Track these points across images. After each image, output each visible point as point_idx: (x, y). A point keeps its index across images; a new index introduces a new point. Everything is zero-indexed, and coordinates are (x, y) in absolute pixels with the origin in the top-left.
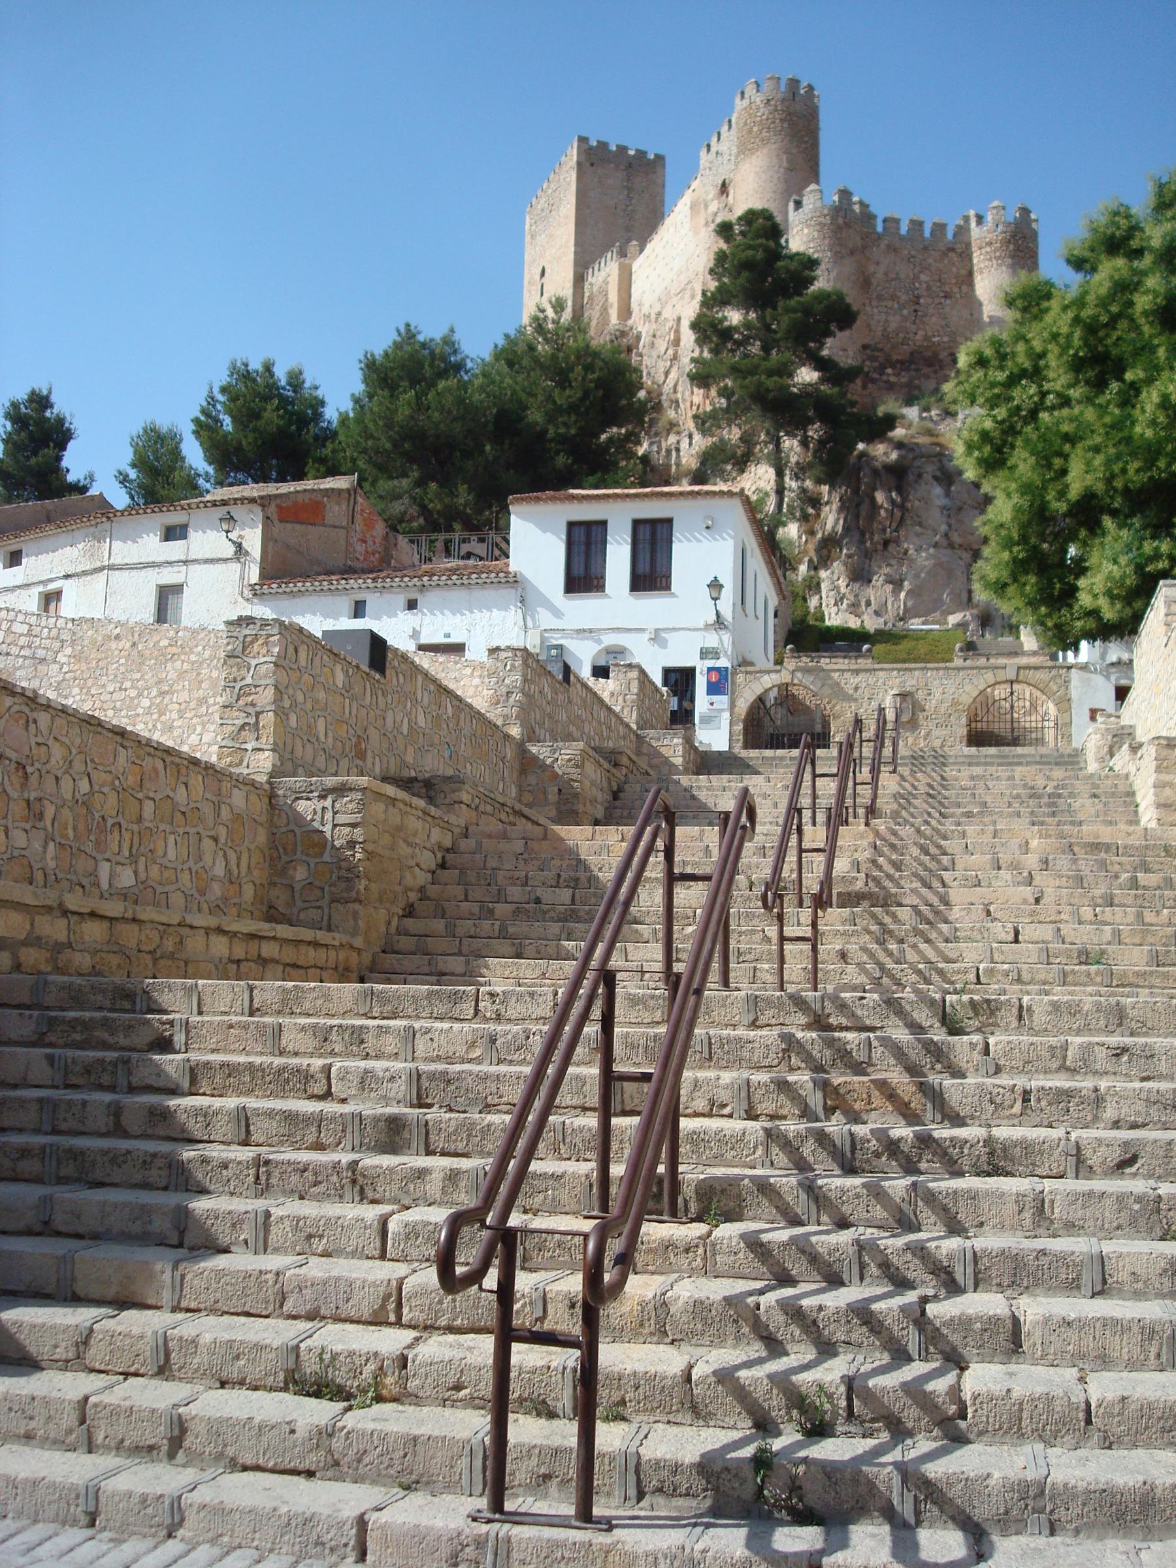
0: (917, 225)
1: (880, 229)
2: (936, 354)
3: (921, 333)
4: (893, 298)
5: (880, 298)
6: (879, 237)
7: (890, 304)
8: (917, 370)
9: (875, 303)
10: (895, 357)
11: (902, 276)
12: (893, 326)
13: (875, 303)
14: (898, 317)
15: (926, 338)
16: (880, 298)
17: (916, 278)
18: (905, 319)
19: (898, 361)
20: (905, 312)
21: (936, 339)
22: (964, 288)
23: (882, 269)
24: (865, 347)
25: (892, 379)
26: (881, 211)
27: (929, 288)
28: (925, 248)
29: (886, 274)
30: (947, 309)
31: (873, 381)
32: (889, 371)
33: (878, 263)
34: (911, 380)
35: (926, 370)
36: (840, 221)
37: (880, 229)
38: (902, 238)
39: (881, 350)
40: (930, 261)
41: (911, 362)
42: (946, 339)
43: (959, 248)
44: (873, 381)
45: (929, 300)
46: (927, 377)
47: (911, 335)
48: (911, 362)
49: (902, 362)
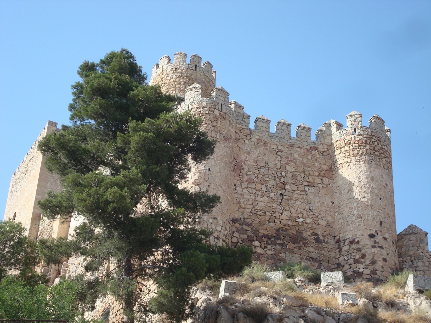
0: (284, 126)
1: (252, 126)
2: (300, 233)
3: (286, 213)
4: (262, 182)
5: (249, 181)
6: (251, 132)
7: (259, 186)
8: (282, 245)
9: (245, 185)
10: (262, 232)
11: (271, 165)
12: (261, 205)
13: (245, 185)
14: (265, 198)
16: (249, 181)
17: (282, 168)
18: (273, 200)
19: (264, 236)
20: (272, 195)
21: (301, 220)
22: (326, 180)
24: (234, 221)
26: (253, 111)
27: (294, 177)
28: (292, 145)
30: (311, 196)
32: (256, 243)
33: (249, 153)
34: (277, 253)
35: (291, 246)
37: (252, 126)
38: (271, 135)
39: (250, 225)
40: (296, 156)
42: (309, 221)
43: (321, 148)
45: (295, 188)
46: (292, 252)
47: (277, 214)
48: (277, 237)
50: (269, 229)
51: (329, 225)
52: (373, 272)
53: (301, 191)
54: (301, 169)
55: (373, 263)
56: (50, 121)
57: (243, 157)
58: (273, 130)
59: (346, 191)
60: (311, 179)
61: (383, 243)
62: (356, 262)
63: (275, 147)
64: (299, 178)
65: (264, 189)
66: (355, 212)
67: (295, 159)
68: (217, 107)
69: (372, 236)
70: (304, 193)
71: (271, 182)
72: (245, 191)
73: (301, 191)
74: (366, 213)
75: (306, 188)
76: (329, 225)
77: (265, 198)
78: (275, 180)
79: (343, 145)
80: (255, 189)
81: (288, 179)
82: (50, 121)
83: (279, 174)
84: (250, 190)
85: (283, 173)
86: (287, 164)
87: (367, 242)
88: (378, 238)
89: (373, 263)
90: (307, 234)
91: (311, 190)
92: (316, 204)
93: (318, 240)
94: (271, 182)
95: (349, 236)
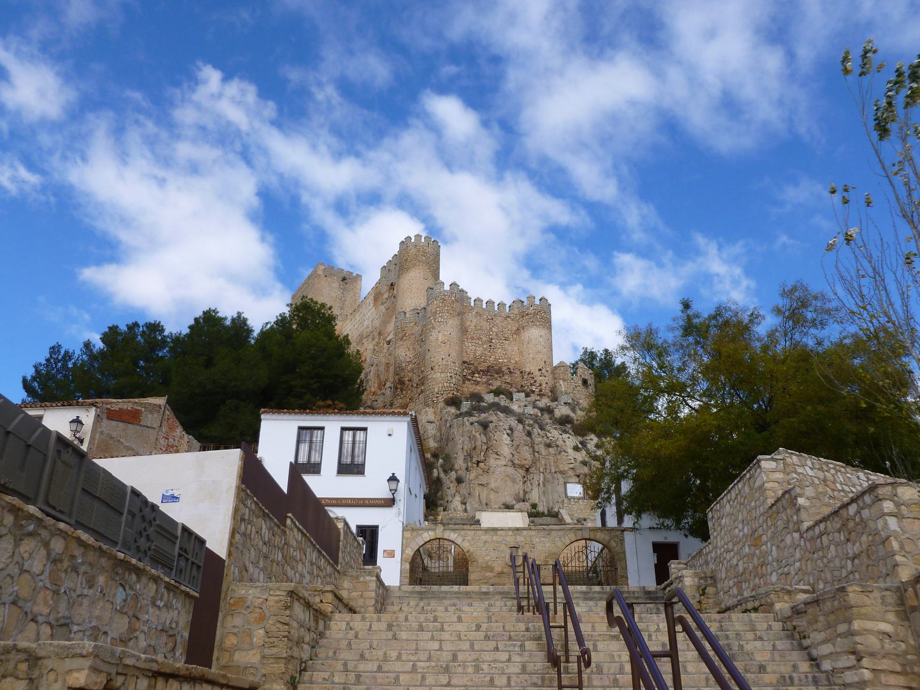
0: (490, 303)
1: (472, 304)
2: (500, 368)
4: (479, 339)
5: (472, 338)
6: (472, 308)
10: (479, 368)
12: (478, 353)
15: (496, 360)
16: (472, 338)
17: (491, 329)
18: (485, 350)
23: (473, 324)
24: (464, 362)
25: (478, 379)
26: (473, 295)
27: (497, 335)
31: (469, 380)
34: (487, 381)
37: (472, 304)
38: (483, 309)
41: (488, 371)
44: (469, 380)
46: (496, 379)
48: (488, 371)
49: (483, 371)
50: (483, 367)
51: (516, 363)
52: (541, 391)
55: (540, 385)
56: (377, 527)
57: (468, 323)
58: (484, 306)
61: (546, 374)
62: (531, 385)
69: (540, 370)
76: (516, 363)
82: (377, 527)
87: (538, 373)
88: (544, 371)
89: (540, 385)
90: (504, 369)
93: (510, 372)
95: (528, 370)
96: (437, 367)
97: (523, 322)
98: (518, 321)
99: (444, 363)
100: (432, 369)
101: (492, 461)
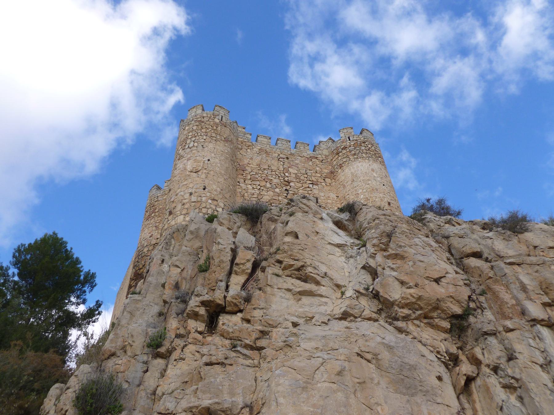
7: (263, 183)
11: (273, 168)
14: (271, 193)
17: (286, 170)
20: (277, 190)
27: (297, 177)
29: (259, 165)
36: (217, 121)
53: (306, 188)
54: (304, 172)
59: (350, 183)
60: (313, 179)
63: (277, 155)
64: (302, 178)
65: (268, 185)
66: (362, 196)
67: (297, 164)
68: (217, 117)
70: (308, 189)
71: (276, 181)
72: (249, 187)
73: (306, 188)
74: (372, 196)
75: (311, 186)
77: (271, 193)
78: (279, 179)
79: (340, 150)
80: (259, 185)
81: (292, 178)
83: (283, 175)
84: (255, 187)
85: (287, 174)
86: (289, 167)
91: (315, 187)
92: (322, 198)
94: (276, 181)
96: (179, 207)
97: (340, 159)
98: (331, 163)
99: (194, 199)
100: (171, 213)
101: (279, 302)
